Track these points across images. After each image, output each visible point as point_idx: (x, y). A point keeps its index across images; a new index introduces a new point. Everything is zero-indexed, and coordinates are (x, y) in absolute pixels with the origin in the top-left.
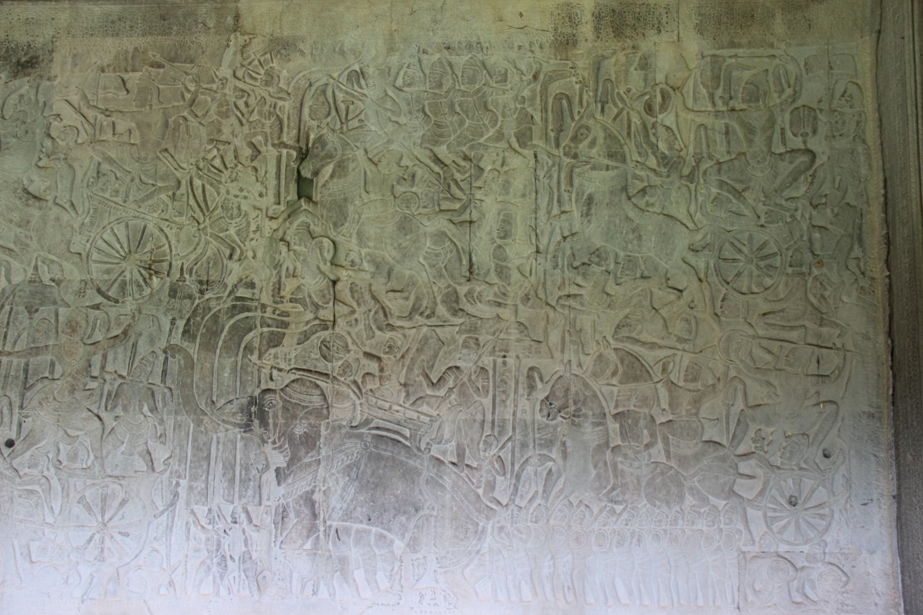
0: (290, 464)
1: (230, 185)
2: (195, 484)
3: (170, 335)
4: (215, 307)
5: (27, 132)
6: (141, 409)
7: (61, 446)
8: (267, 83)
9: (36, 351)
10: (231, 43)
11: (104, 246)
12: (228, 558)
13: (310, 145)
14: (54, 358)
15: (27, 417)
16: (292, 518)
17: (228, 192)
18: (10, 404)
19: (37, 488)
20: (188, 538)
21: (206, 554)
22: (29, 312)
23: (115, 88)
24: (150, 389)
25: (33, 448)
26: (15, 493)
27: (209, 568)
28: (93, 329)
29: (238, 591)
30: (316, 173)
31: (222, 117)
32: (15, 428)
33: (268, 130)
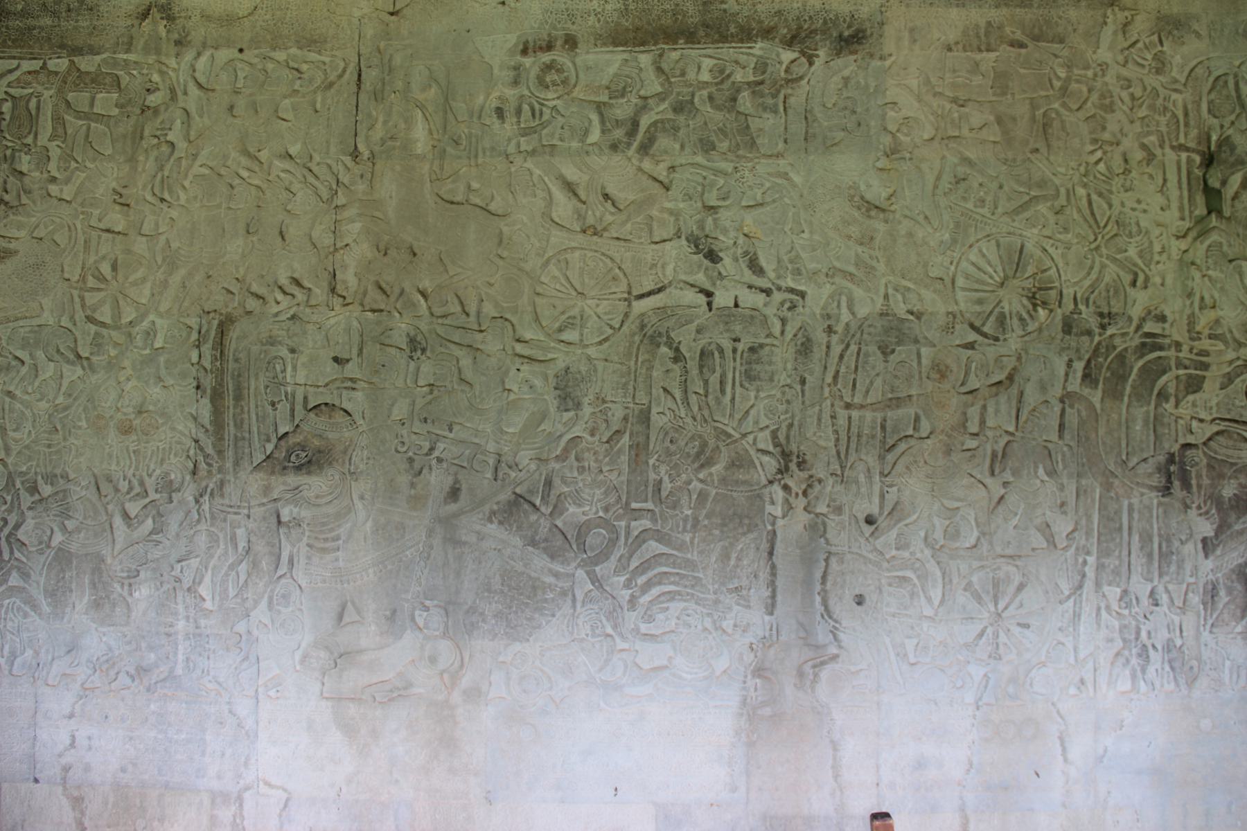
0: (1219, 531)
1: (1124, 195)
2: (1106, 561)
3: (1066, 381)
4: (1120, 345)
5: (859, 125)
6: (1036, 472)
7: (936, 521)
8: (1159, 71)
9: (897, 402)
10: (1108, 20)
11: (972, 270)
12: (1150, 648)
13: (1213, 148)
14: (921, 413)
15: (891, 486)
16: (1223, 597)
17: (1123, 204)
18: (869, 470)
19: (909, 574)
20: (1099, 625)
21: (1121, 644)
22: (884, 353)
23: (968, 71)
24: (1046, 447)
25: (901, 524)
26: (883, 581)
27: (1128, 661)
28: (967, 374)
29: (1162, 686)
30: (1224, 183)
31: (1106, 111)
32: (876, 500)
33: (1163, 129)
